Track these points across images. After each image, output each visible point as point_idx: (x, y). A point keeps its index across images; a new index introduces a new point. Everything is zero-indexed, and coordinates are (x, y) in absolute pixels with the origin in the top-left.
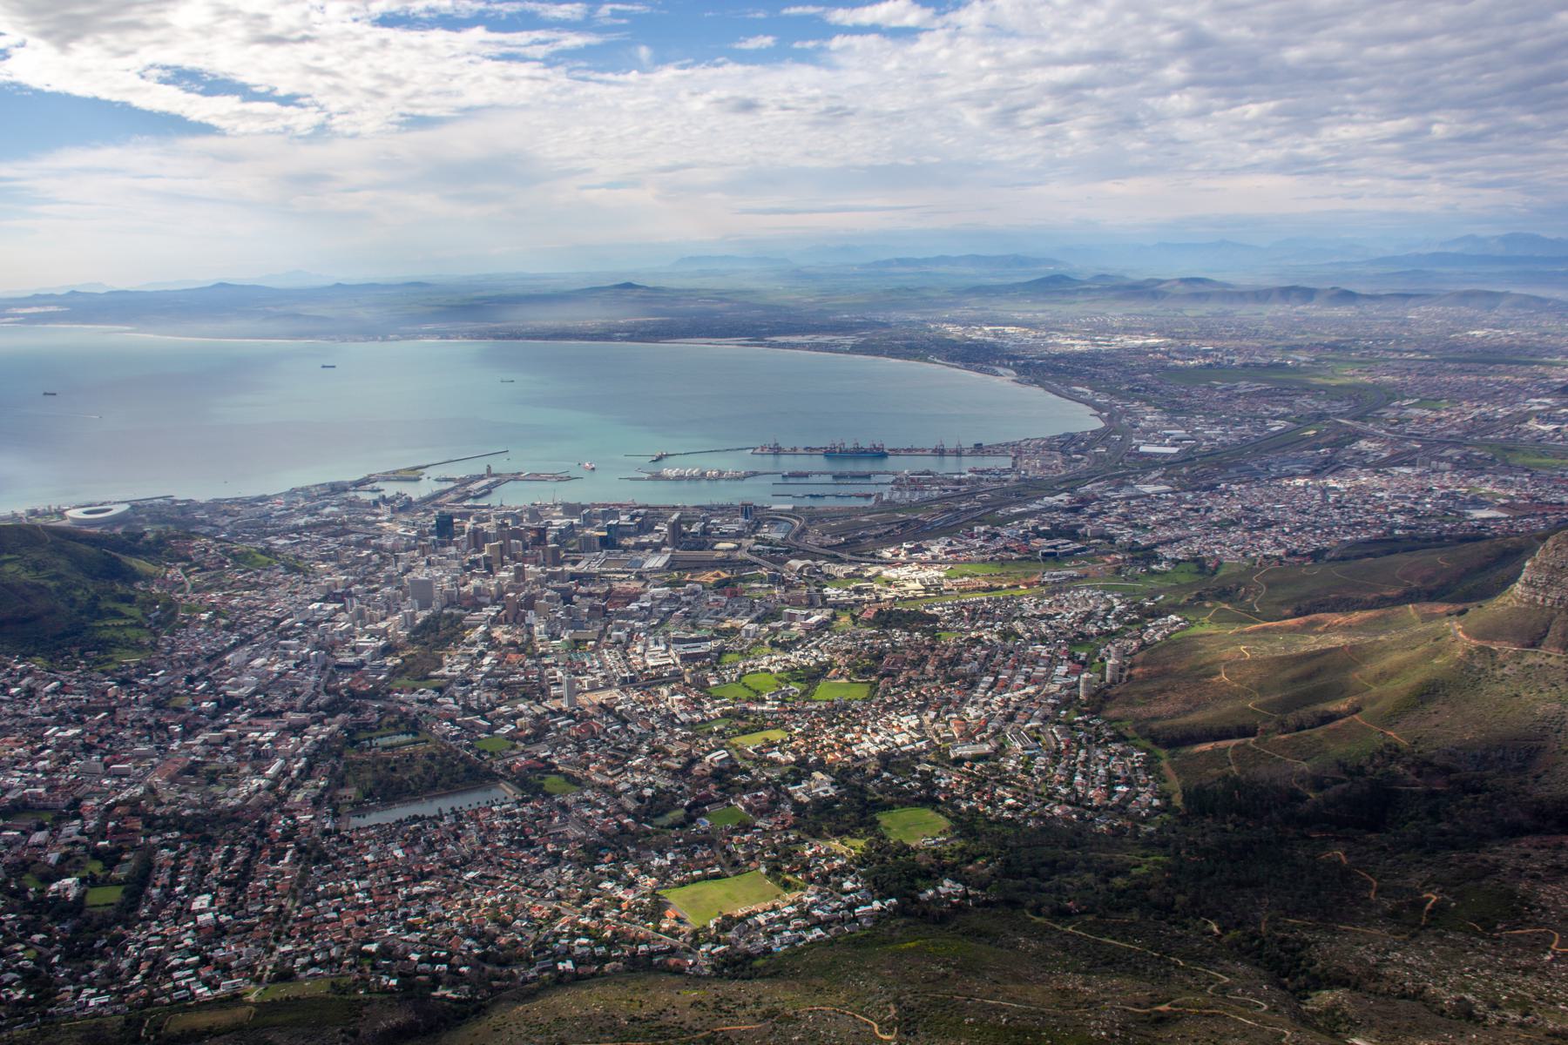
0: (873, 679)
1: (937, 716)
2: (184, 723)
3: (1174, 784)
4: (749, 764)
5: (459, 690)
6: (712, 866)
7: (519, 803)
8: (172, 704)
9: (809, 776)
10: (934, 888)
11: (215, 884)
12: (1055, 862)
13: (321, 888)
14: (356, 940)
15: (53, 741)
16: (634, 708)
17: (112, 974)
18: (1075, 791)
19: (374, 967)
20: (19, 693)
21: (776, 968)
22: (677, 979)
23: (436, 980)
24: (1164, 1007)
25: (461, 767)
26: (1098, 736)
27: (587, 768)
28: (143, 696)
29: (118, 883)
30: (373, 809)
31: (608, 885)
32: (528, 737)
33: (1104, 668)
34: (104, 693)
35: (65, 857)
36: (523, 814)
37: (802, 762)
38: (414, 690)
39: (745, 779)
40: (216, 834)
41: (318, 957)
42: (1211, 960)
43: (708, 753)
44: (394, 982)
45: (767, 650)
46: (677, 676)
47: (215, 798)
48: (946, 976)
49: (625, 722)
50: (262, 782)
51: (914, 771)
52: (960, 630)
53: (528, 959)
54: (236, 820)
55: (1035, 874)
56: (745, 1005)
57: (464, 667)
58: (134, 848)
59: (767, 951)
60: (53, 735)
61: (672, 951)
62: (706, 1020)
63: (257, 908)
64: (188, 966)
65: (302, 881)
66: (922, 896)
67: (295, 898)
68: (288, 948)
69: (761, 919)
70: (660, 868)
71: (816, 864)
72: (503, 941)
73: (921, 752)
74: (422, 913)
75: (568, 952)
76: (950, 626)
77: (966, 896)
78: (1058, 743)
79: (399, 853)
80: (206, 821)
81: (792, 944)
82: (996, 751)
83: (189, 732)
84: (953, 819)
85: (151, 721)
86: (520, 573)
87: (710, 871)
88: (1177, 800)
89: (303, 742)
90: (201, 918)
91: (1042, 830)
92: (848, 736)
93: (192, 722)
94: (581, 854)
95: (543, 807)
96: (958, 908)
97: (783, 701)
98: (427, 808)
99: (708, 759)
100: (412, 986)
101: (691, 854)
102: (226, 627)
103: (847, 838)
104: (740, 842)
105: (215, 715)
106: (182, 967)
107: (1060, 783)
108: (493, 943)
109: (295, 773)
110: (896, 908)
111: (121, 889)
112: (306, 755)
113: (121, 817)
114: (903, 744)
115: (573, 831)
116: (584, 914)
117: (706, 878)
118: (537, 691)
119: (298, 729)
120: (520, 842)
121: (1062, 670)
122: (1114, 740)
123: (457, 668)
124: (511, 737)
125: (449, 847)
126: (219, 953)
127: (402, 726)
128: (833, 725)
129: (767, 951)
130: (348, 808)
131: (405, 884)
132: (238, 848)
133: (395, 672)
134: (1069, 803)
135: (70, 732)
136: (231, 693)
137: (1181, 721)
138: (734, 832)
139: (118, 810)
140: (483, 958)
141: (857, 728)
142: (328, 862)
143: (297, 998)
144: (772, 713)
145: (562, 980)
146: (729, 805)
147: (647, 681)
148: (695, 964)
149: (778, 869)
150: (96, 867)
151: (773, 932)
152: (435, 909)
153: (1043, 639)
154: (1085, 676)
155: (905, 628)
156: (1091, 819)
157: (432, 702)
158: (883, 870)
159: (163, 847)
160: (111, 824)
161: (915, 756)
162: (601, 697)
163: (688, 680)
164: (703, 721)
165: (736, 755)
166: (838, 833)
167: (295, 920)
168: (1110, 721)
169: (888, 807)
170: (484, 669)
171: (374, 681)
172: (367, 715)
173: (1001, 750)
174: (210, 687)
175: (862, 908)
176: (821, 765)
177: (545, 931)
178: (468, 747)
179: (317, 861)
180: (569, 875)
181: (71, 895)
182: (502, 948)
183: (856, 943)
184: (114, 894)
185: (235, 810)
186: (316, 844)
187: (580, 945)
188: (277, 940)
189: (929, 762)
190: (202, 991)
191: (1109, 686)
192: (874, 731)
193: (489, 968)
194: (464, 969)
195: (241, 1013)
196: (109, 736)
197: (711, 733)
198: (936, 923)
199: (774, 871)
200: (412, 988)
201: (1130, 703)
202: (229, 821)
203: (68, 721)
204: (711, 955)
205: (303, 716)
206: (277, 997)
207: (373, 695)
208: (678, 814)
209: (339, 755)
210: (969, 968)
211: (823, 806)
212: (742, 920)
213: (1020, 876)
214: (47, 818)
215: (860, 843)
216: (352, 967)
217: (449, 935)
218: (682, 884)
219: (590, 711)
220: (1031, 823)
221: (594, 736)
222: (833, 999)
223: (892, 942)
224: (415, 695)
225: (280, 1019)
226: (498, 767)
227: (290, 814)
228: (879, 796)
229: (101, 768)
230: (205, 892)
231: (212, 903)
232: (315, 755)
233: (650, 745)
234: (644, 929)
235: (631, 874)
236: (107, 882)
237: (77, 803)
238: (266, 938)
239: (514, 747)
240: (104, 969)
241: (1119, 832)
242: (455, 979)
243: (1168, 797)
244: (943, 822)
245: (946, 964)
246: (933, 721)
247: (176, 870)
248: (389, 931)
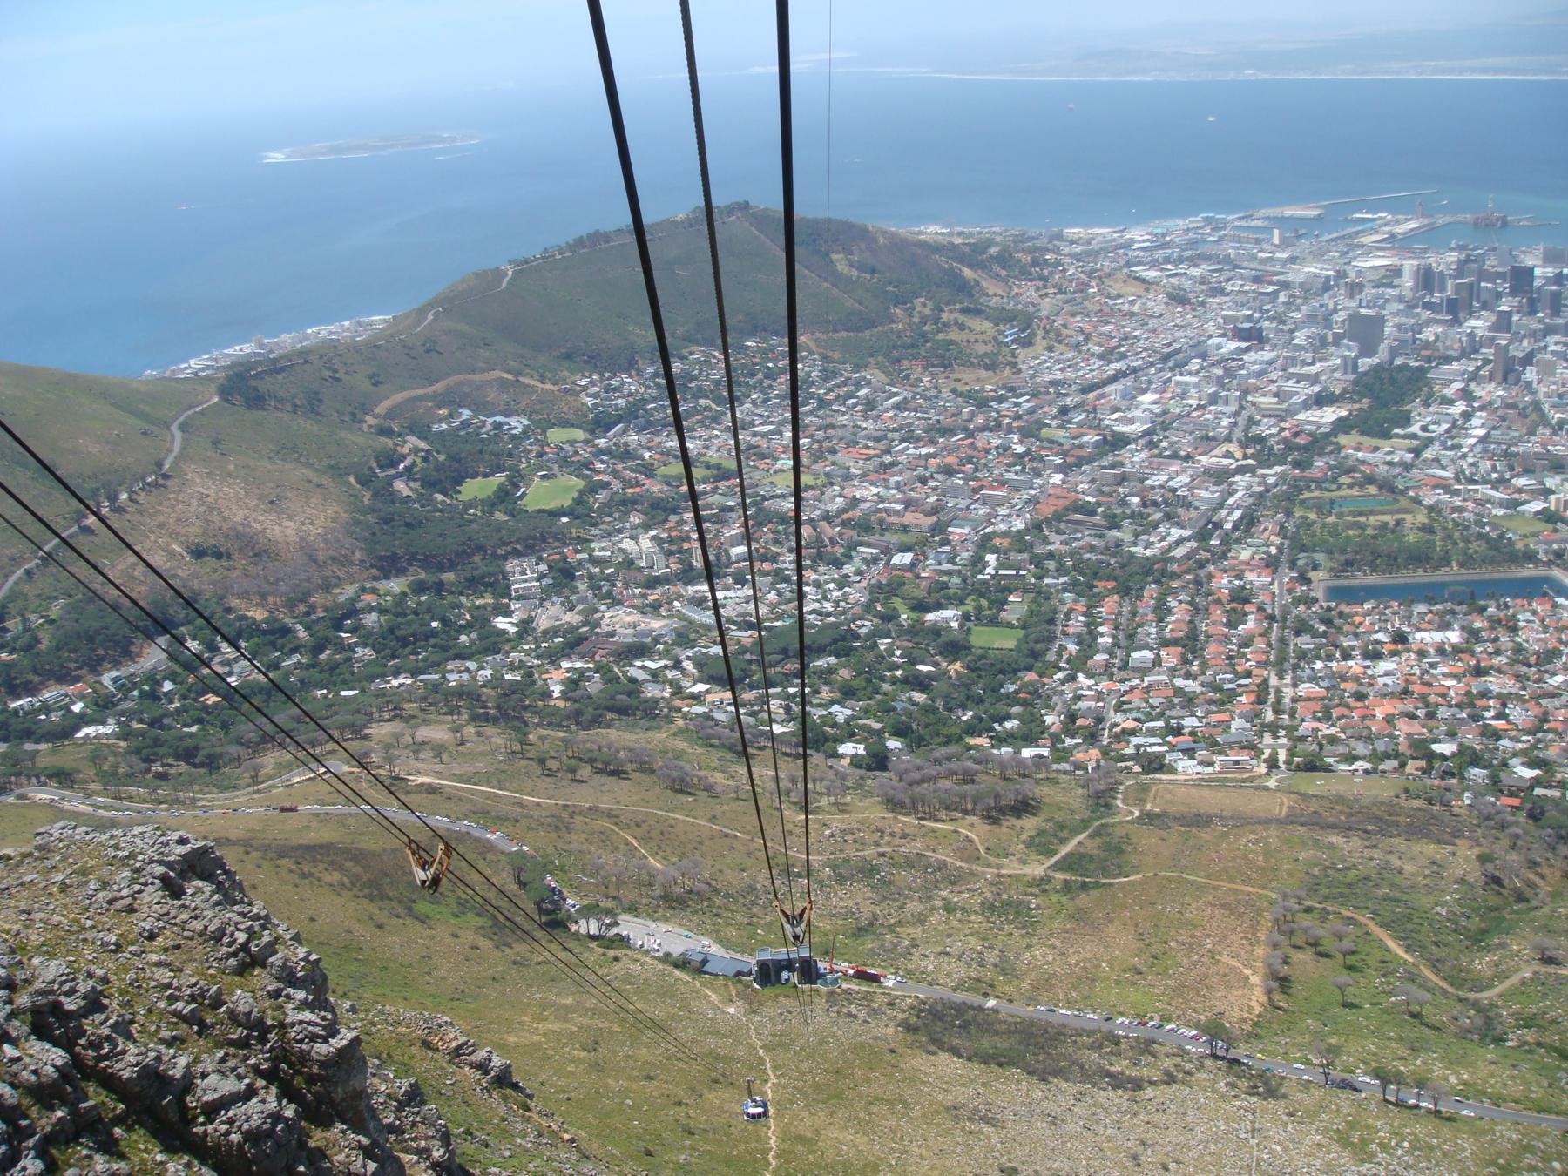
20: (855, 405)
29: (1012, 626)
38: (1376, 449)
60: (902, 452)
64: (1151, 732)
86: (1503, 323)
102: (1101, 357)
109: (1228, 526)
111: (1021, 633)
133: (1341, 426)
170: (1481, 432)
231: (1157, 662)
236: (994, 621)
237: (939, 529)
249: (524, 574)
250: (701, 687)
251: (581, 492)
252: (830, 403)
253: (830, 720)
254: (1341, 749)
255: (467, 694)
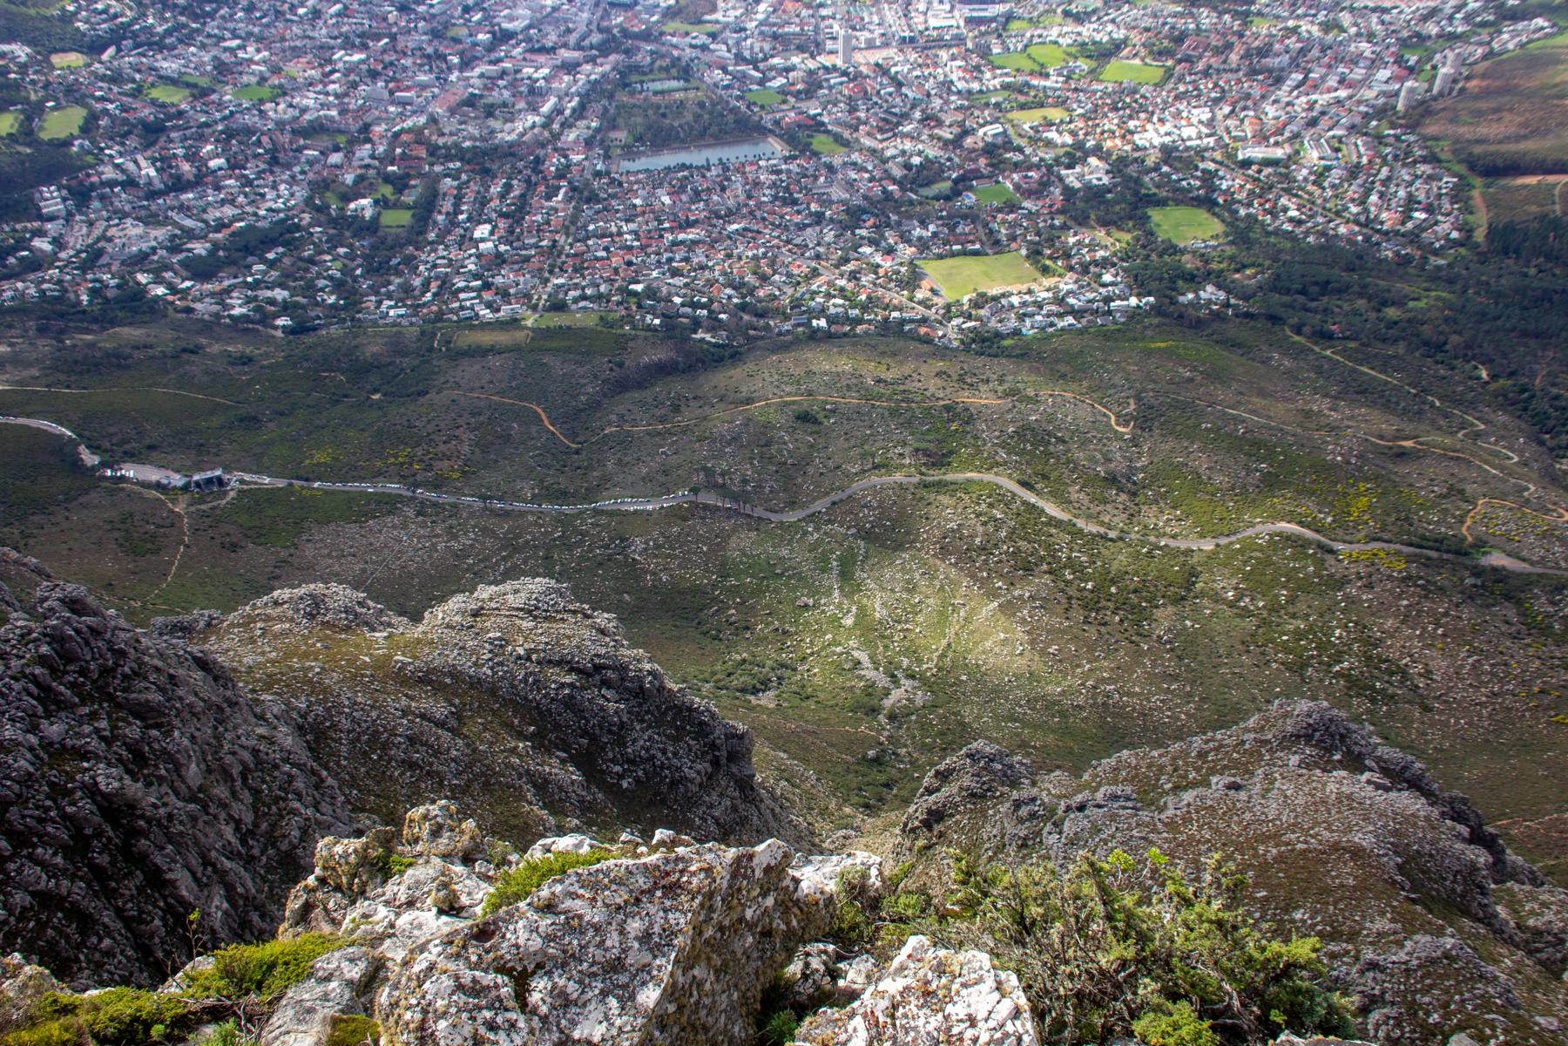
0: (1170, 63)
1: (1232, 112)
2: (461, 54)
3: (1481, 220)
4: (1023, 142)
5: (732, 37)
6: (973, 242)
7: (786, 159)
8: (449, 34)
9: (1083, 161)
10: (1196, 292)
11: (494, 216)
12: (1328, 282)
13: (591, 227)
14: (623, 279)
15: (340, 65)
16: (910, 71)
17: (407, 289)
18: (1366, 211)
19: (640, 306)
21: (1025, 353)
22: (925, 348)
23: (696, 324)
24: (1408, 444)
25: (731, 118)
26: (1408, 154)
27: (856, 130)
28: (421, 24)
29: (408, 207)
30: (643, 153)
31: (867, 250)
32: (799, 92)
33: (1434, 77)
34: (385, 19)
35: (361, 179)
36: (789, 171)
37: (1079, 146)
38: (687, 34)
39: (1018, 157)
40: (495, 167)
41: (589, 292)
42: (1471, 405)
43: (982, 126)
44: (657, 321)
45: (1059, 18)
46: (959, 40)
47: (492, 132)
48: (1191, 380)
49: (900, 85)
50: (537, 119)
51: (1196, 168)
52: (1277, 17)
53: (784, 313)
54: (513, 155)
55: (1303, 292)
56: (988, 381)
57: (738, 13)
58: (421, 175)
59: (1017, 332)
61: (924, 321)
62: (948, 391)
63: (533, 241)
65: (574, 219)
66: (1181, 299)
67: (567, 235)
68: (561, 281)
69: (1015, 300)
70: (920, 238)
71: (1078, 253)
72: (761, 293)
73: (1206, 149)
74: (687, 260)
75: (823, 311)
76: (1266, 11)
77: (1227, 305)
78: (1360, 156)
79: (666, 200)
80: (485, 153)
81: (1043, 329)
82: (1289, 157)
83: (466, 64)
84: (1228, 224)
85: (430, 50)
87: (970, 247)
88: (1480, 236)
89: (576, 81)
90: (482, 246)
91: (1322, 247)
92: (1132, 124)
93: (469, 54)
94: (843, 217)
95: (810, 165)
96: (1217, 316)
97: (1069, 78)
98: (695, 157)
99: (981, 132)
100: (674, 328)
101: (952, 228)
103: (1113, 230)
104: (1004, 222)
105: (491, 48)
106: (466, 289)
107: (1353, 200)
108: (752, 295)
109: (568, 112)
110: (1152, 307)
111: (410, 213)
112: (579, 95)
113: (406, 145)
114: (1190, 139)
115: (837, 193)
116: (842, 275)
117: (965, 253)
118: (811, 46)
119: (570, 68)
120: (784, 199)
121: (1384, 74)
122: (1424, 160)
123: (732, 13)
124: (782, 91)
125: (715, 198)
126: (499, 280)
127: (674, 72)
128: (1116, 109)
129: (1017, 332)
130: (619, 151)
131: (671, 230)
132: (515, 182)
134: (1357, 223)
135: (357, 57)
136: (506, 25)
137: (1505, 148)
138: (999, 210)
139: (404, 137)
140: (743, 307)
141: (1143, 116)
142: (598, 202)
143: (569, 328)
144: (1056, 90)
145: (814, 336)
146: (998, 182)
147: (926, 44)
148: (944, 336)
149: (1039, 253)
150: (387, 190)
151: (1025, 315)
152: (699, 257)
153: (1370, 36)
154: (1409, 84)
155: (1215, 9)
156: (1378, 244)
157: (704, 48)
158: (1146, 267)
159: (447, 176)
160: (399, 151)
161: (1200, 153)
162: (877, 56)
163: (970, 45)
164: (981, 92)
165: (1011, 132)
166: (1105, 223)
167: (568, 256)
168: (1425, 138)
169: (1161, 203)
170: (760, 17)
171: (647, 22)
172: (639, 57)
173: (1294, 157)
174: (485, 19)
175: (1118, 303)
176: (1098, 151)
177: (802, 289)
178: (739, 98)
179: (588, 201)
180: (829, 236)
181: (368, 214)
182: (760, 301)
183: (1105, 335)
184: (405, 217)
185: (511, 145)
186: (587, 184)
187: (835, 306)
188: (551, 272)
189: (1213, 161)
190: (485, 313)
191: (1435, 99)
192: (1160, 120)
193: (746, 317)
194: (722, 316)
195: (520, 336)
196: (392, 64)
197: (987, 105)
198: (1191, 327)
199: (1035, 254)
200: (674, 329)
201: (1454, 121)
202: (506, 155)
203: (353, 46)
204: (961, 329)
205: (576, 54)
206: (552, 325)
207: (646, 36)
208: (944, 186)
209: (611, 97)
210: (1216, 376)
211: (1095, 194)
212: (995, 299)
213: (1288, 292)
214: (341, 140)
215: (1127, 237)
216: (619, 303)
217: (710, 283)
218: (940, 257)
219: (864, 70)
220: (1311, 239)
221: (866, 96)
222: (1075, 386)
223: (1143, 339)
224: (688, 40)
225: (554, 345)
226: (767, 120)
227: (563, 153)
228: (1154, 190)
229: (386, 95)
230: (485, 222)
231: (492, 233)
232: (587, 95)
233: (923, 111)
234: (898, 297)
235: (891, 241)
236: (397, 205)
237: (366, 128)
238: (541, 270)
239: (784, 102)
240: (400, 285)
241: (1405, 261)
242: (714, 325)
243: (1470, 231)
244: (1217, 227)
245: (1194, 369)
246: (1226, 117)
247: (459, 199)
248: (655, 274)
249: (52, 199)
250: (188, 284)
251: (86, 120)
252: (283, 14)
253: (272, 302)
254: (577, 293)
255: (22, 309)
